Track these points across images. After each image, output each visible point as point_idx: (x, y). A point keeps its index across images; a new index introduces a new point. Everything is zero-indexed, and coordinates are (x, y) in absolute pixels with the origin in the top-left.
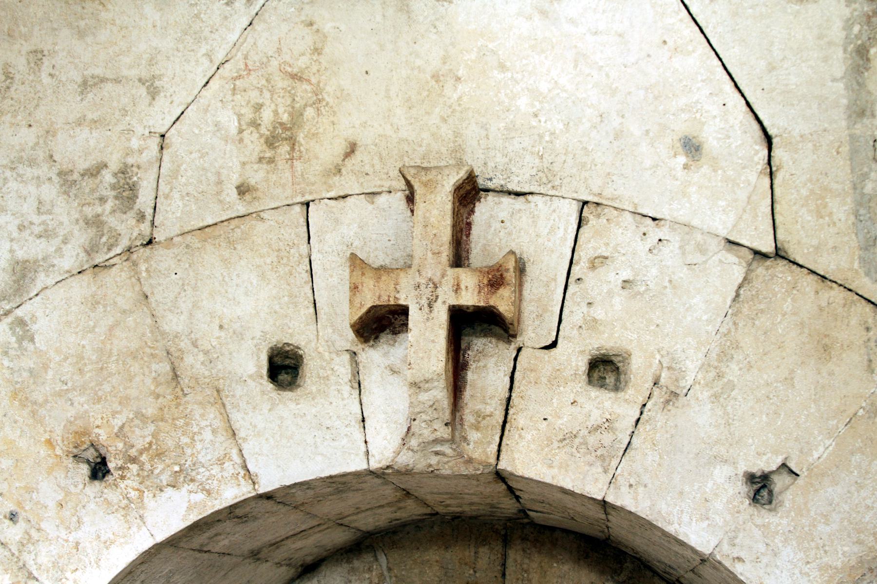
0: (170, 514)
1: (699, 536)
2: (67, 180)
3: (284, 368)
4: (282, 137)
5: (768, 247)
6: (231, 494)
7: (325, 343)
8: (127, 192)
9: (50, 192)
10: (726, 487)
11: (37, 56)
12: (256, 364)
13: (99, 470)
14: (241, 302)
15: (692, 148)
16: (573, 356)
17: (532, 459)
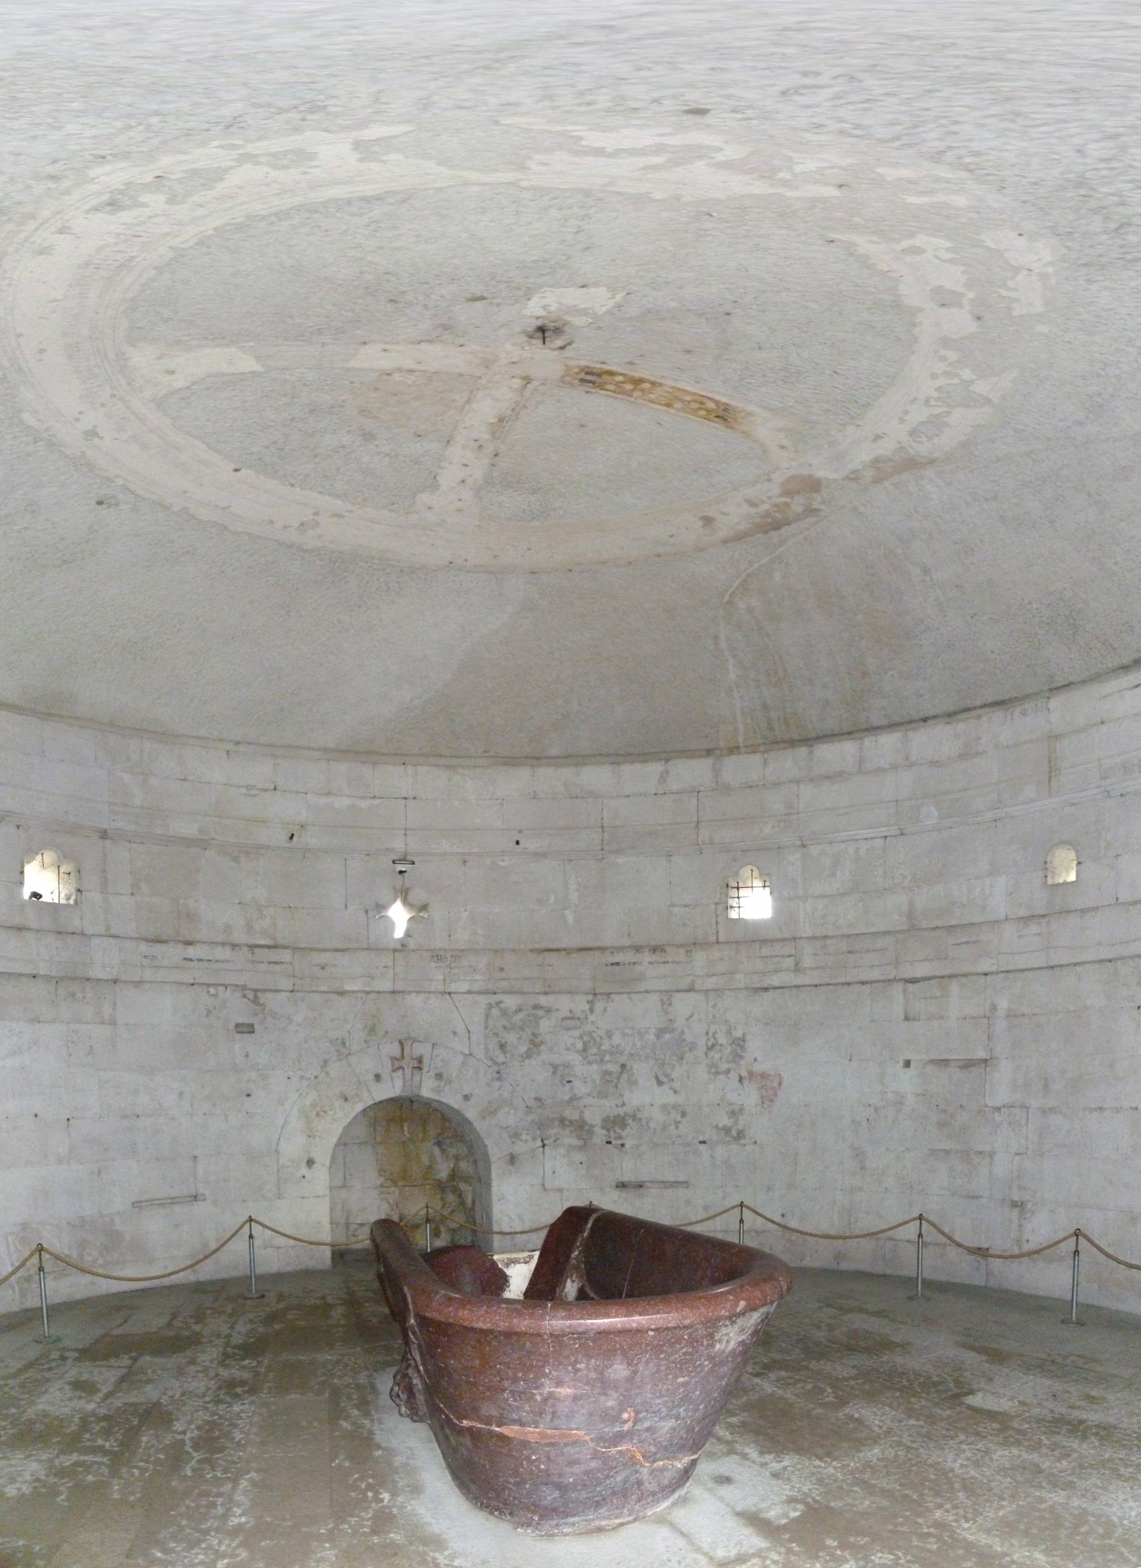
0: (359, 1107)
1: (456, 1106)
2: (331, 1042)
3: (378, 1077)
5: (467, 1051)
6: (370, 1102)
7: (385, 1072)
8: (344, 1044)
9: (328, 1044)
10: (459, 1098)
11: (321, 1015)
12: (371, 1077)
13: (346, 1100)
14: (367, 1064)
15: (455, 1033)
16: (432, 1073)
17: (427, 1092)
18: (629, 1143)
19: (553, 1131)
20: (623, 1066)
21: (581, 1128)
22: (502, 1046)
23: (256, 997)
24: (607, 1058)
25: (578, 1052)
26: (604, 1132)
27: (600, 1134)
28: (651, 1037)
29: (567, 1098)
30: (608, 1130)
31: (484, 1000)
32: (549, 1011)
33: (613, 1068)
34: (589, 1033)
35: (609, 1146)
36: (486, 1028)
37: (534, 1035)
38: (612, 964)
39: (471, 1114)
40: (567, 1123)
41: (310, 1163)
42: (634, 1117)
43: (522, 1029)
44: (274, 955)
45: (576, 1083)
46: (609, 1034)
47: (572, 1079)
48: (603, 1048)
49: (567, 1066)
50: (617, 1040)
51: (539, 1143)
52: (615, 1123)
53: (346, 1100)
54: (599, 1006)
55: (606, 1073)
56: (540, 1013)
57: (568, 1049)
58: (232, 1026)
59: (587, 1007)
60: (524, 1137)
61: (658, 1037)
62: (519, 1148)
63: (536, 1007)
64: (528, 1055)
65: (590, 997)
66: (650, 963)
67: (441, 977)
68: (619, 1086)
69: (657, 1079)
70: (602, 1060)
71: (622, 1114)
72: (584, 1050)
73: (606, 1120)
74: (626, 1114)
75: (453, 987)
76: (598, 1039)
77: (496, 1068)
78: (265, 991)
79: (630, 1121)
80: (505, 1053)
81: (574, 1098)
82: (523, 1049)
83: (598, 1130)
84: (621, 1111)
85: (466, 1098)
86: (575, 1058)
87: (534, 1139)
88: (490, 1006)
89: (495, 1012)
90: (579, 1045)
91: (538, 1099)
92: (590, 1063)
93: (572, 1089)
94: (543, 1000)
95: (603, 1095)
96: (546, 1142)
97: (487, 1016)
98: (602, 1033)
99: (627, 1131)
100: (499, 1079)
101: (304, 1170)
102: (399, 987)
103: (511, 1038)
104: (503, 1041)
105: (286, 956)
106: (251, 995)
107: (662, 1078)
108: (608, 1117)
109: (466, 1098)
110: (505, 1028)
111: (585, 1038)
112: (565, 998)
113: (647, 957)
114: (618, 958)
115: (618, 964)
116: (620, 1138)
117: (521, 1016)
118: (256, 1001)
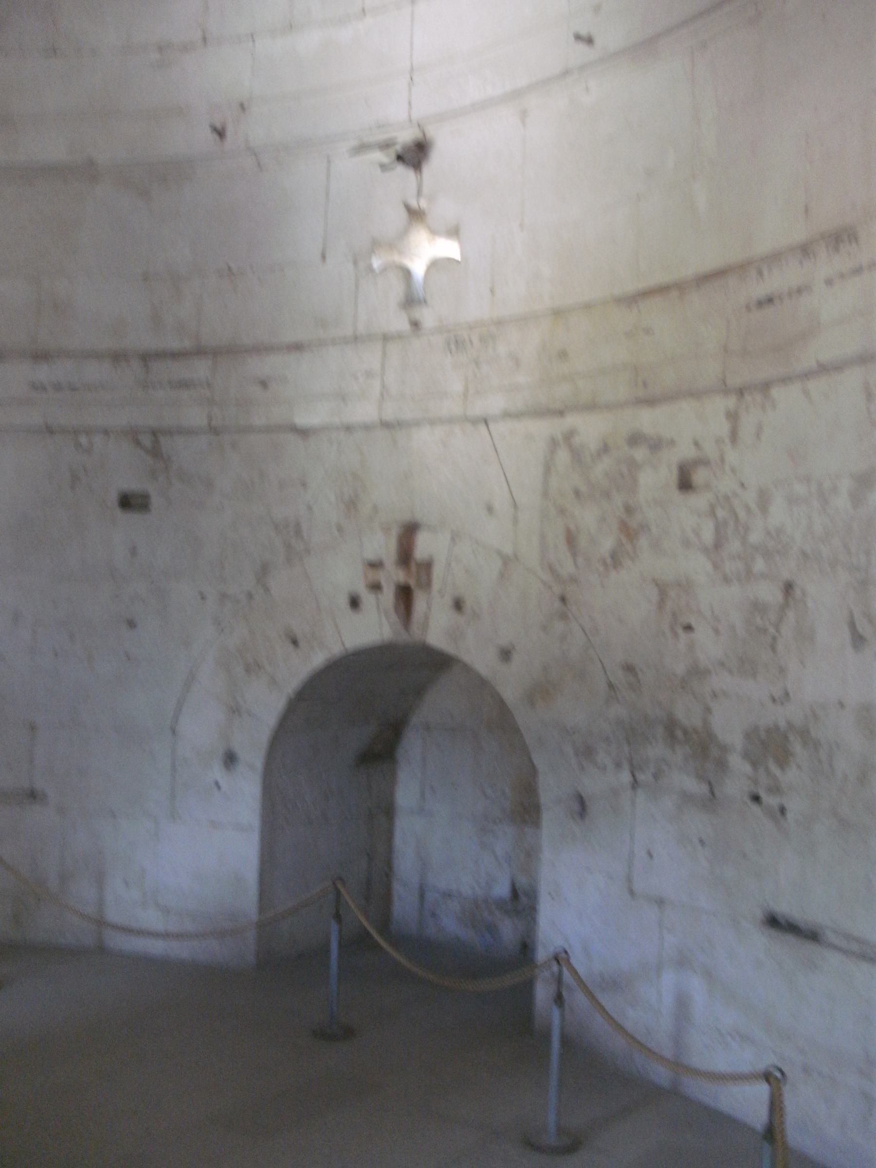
0: (318, 659)
3: (355, 603)
4: (351, 505)
8: (298, 532)
13: (295, 642)
15: (490, 509)
18: (795, 805)
19: (656, 750)
20: (788, 588)
21: (704, 749)
22: (571, 539)
23: (156, 442)
24: (759, 565)
25: (706, 550)
26: (747, 768)
27: (739, 775)
28: (841, 502)
29: (680, 669)
30: (755, 764)
31: (542, 429)
32: (656, 445)
33: (769, 593)
34: (727, 498)
35: (755, 808)
36: (545, 494)
37: (629, 510)
38: (760, 304)
39: (510, 693)
40: (679, 733)
41: (230, 759)
42: (804, 734)
43: (607, 495)
44: (178, 370)
45: (703, 635)
46: (764, 500)
47: (693, 620)
48: (755, 537)
49: (686, 586)
50: (778, 513)
51: (625, 777)
52: (772, 746)
53: (295, 642)
54: (747, 424)
55: (757, 607)
56: (640, 454)
57: (686, 543)
58: (113, 497)
59: (722, 427)
60: (601, 757)
61: (857, 499)
62: (593, 783)
63: (635, 439)
64: (615, 560)
65: (731, 402)
66: (829, 282)
67: (457, 387)
68: (780, 647)
69: (852, 625)
70: (749, 572)
71: (782, 724)
72: (718, 545)
73: (751, 734)
74: (790, 725)
75: (478, 408)
76: (742, 514)
77: (557, 590)
78: (169, 432)
79: (797, 747)
80: (574, 555)
81: (697, 672)
82: (607, 544)
83: (737, 763)
84: (780, 716)
85: (506, 654)
86: (697, 566)
87: (618, 765)
88: (553, 444)
89: (563, 456)
90: (708, 535)
91: (629, 668)
92: (726, 580)
93: (691, 646)
94: (648, 420)
95: (747, 666)
96: (641, 777)
97: (548, 469)
98: (750, 497)
99: (791, 776)
100: (564, 617)
101: (217, 772)
102: (389, 414)
103: (587, 517)
104: (572, 527)
105: (201, 369)
106: (147, 440)
107: (864, 627)
108: (756, 729)
109: (506, 654)
110: (577, 493)
111: (721, 513)
112: (686, 407)
113: (825, 265)
114: (776, 281)
115: (770, 300)
116: (776, 789)
117: (605, 464)
118: (155, 452)
